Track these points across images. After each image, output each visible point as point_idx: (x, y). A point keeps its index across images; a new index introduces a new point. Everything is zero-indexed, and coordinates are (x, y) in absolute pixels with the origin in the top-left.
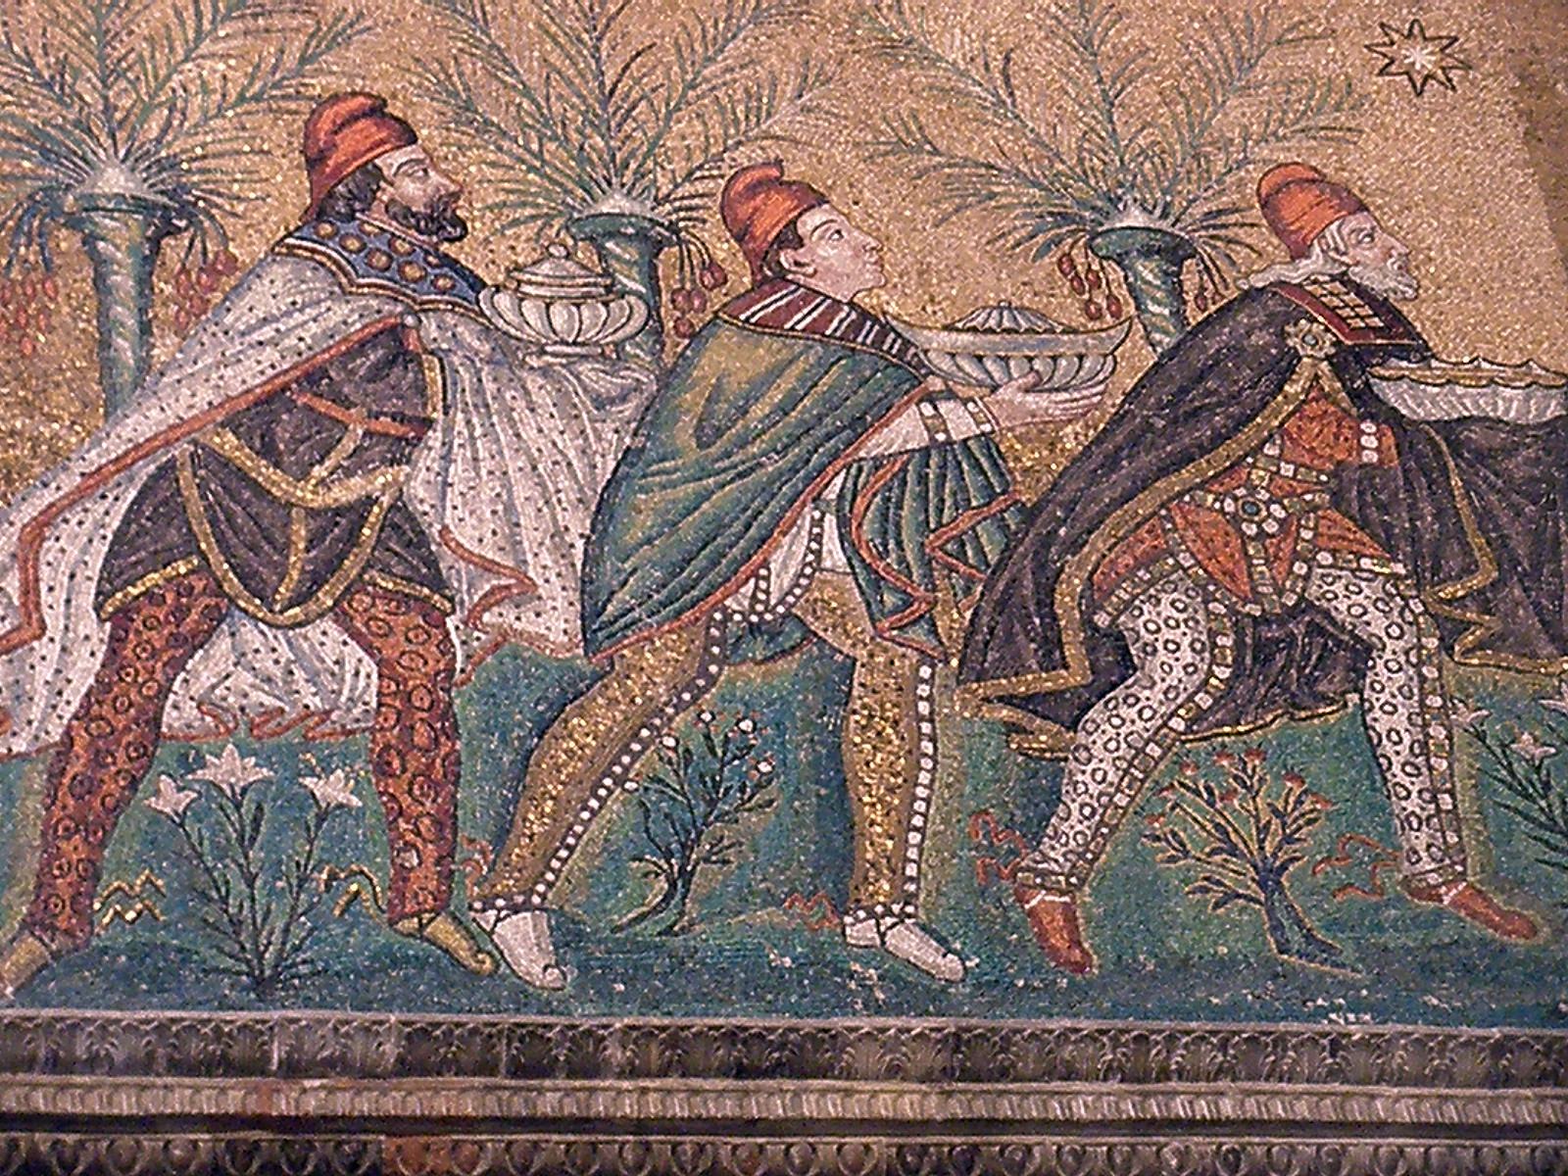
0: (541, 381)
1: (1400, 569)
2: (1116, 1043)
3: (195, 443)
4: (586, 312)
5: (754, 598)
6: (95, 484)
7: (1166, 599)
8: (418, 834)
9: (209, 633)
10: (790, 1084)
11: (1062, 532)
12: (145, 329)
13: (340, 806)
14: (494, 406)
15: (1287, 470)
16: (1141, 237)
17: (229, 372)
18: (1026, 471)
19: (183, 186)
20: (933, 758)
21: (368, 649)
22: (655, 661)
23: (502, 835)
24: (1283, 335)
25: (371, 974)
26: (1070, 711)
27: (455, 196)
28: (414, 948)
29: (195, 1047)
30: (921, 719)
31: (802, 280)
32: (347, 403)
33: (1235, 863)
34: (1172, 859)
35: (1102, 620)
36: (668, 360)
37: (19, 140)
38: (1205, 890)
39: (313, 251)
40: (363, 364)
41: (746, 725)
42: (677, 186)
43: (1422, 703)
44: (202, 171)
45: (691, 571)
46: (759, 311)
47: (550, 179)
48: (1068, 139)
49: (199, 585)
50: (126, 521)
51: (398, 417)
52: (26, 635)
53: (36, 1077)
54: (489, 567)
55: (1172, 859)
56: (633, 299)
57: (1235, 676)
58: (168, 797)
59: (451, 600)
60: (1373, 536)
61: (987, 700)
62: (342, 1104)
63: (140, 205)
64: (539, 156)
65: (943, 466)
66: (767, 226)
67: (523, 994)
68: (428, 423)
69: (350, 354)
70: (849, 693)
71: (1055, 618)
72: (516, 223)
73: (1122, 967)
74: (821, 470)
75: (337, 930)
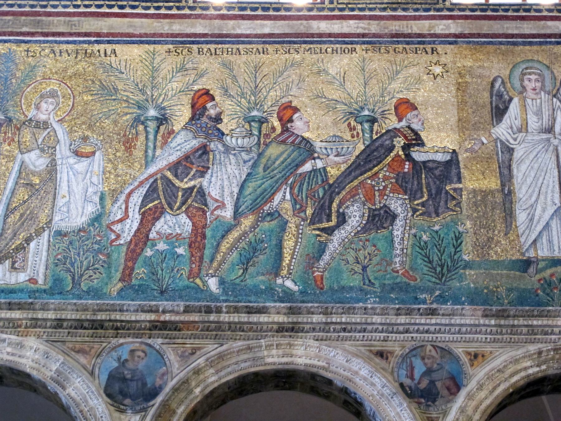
0: (233, 157)
1: (407, 197)
2: (322, 308)
3: (162, 174)
4: (245, 140)
5: (270, 207)
6: (141, 183)
7: (356, 205)
8: (195, 260)
9: (160, 217)
10: (258, 315)
11: (337, 190)
12: (155, 148)
13: (181, 254)
14: (223, 163)
15: (388, 174)
16: (367, 118)
17: (170, 157)
18: (331, 176)
19: (166, 114)
20: (301, 243)
21: (191, 220)
22: (247, 222)
23: (212, 261)
24: (393, 141)
25: (183, 290)
26: (330, 231)
27: (221, 113)
28: (193, 284)
29: (146, 308)
30: (299, 234)
31: (292, 130)
32: (193, 164)
33: (358, 265)
34: (345, 265)
35: (341, 210)
36: (260, 151)
37: (134, 104)
38: (351, 271)
39: (191, 128)
40: (197, 154)
41: (264, 236)
42: (268, 108)
43: (405, 229)
44: (170, 110)
45: (258, 201)
46: (281, 139)
47: (242, 108)
48: (354, 95)
49: (159, 206)
50: (147, 192)
51: (203, 167)
52: (125, 218)
53: (117, 313)
54: (217, 201)
55: (345, 265)
56: (255, 136)
57: (367, 223)
58: (148, 252)
59: (208, 208)
60: (403, 189)
61: (314, 229)
62: (173, 318)
63: (157, 119)
64: (240, 102)
65: (314, 175)
66: (286, 118)
67: (211, 294)
68: (209, 168)
69: (195, 152)
70: (285, 229)
71: (331, 210)
72: (233, 119)
73: (331, 288)
74: (288, 176)
75: (178, 281)
